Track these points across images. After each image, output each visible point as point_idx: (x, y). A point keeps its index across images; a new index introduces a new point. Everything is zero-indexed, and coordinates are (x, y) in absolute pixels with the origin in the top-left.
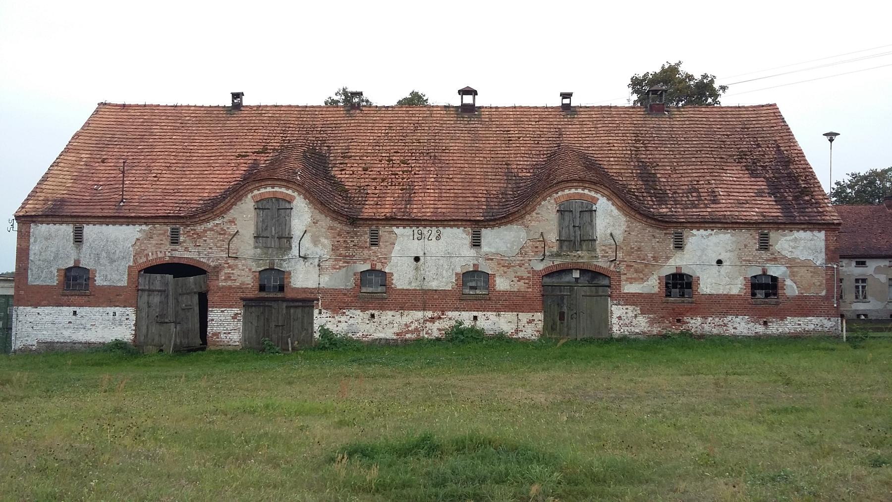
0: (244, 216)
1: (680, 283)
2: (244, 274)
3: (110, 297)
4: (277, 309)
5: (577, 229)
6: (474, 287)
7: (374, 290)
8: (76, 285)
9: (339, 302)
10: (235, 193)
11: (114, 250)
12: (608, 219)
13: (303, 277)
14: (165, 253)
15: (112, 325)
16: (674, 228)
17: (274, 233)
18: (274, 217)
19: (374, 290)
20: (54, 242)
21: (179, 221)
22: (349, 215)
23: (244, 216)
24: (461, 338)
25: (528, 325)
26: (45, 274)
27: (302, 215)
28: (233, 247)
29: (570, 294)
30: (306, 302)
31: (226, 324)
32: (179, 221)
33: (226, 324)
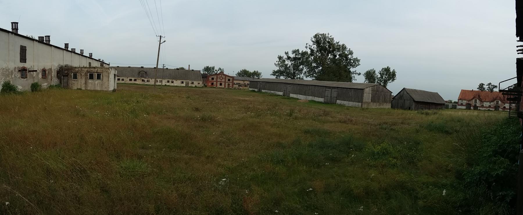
0: (474, 100)
1: (505, 107)
2: (473, 105)
3: (464, 106)
4: (476, 108)
5: (497, 103)
6: (490, 106)
7: (483, 106)
8: (462, 105)
9: (480, 107)
10: (473, 99)
11: (465, 102)
12: (500, 102)
13: (478, 105)
14: (468, 103)
15: (465, 107)
16: (505, 103)
17: (476, 102)
18: (476, 100)
19: (483, 106)
20: (460, 102)
21: (469, 101)
22: (481, 101)
23: (474, 100)
24: (489, 110)
25: (493, 109)
26: (460, 103)
27: (478, 101)
28: (473, 103)
29: (497, 108)
30: (478, 107)
31: (472, 108)
32: (469, 101)
33: (472, 108)
